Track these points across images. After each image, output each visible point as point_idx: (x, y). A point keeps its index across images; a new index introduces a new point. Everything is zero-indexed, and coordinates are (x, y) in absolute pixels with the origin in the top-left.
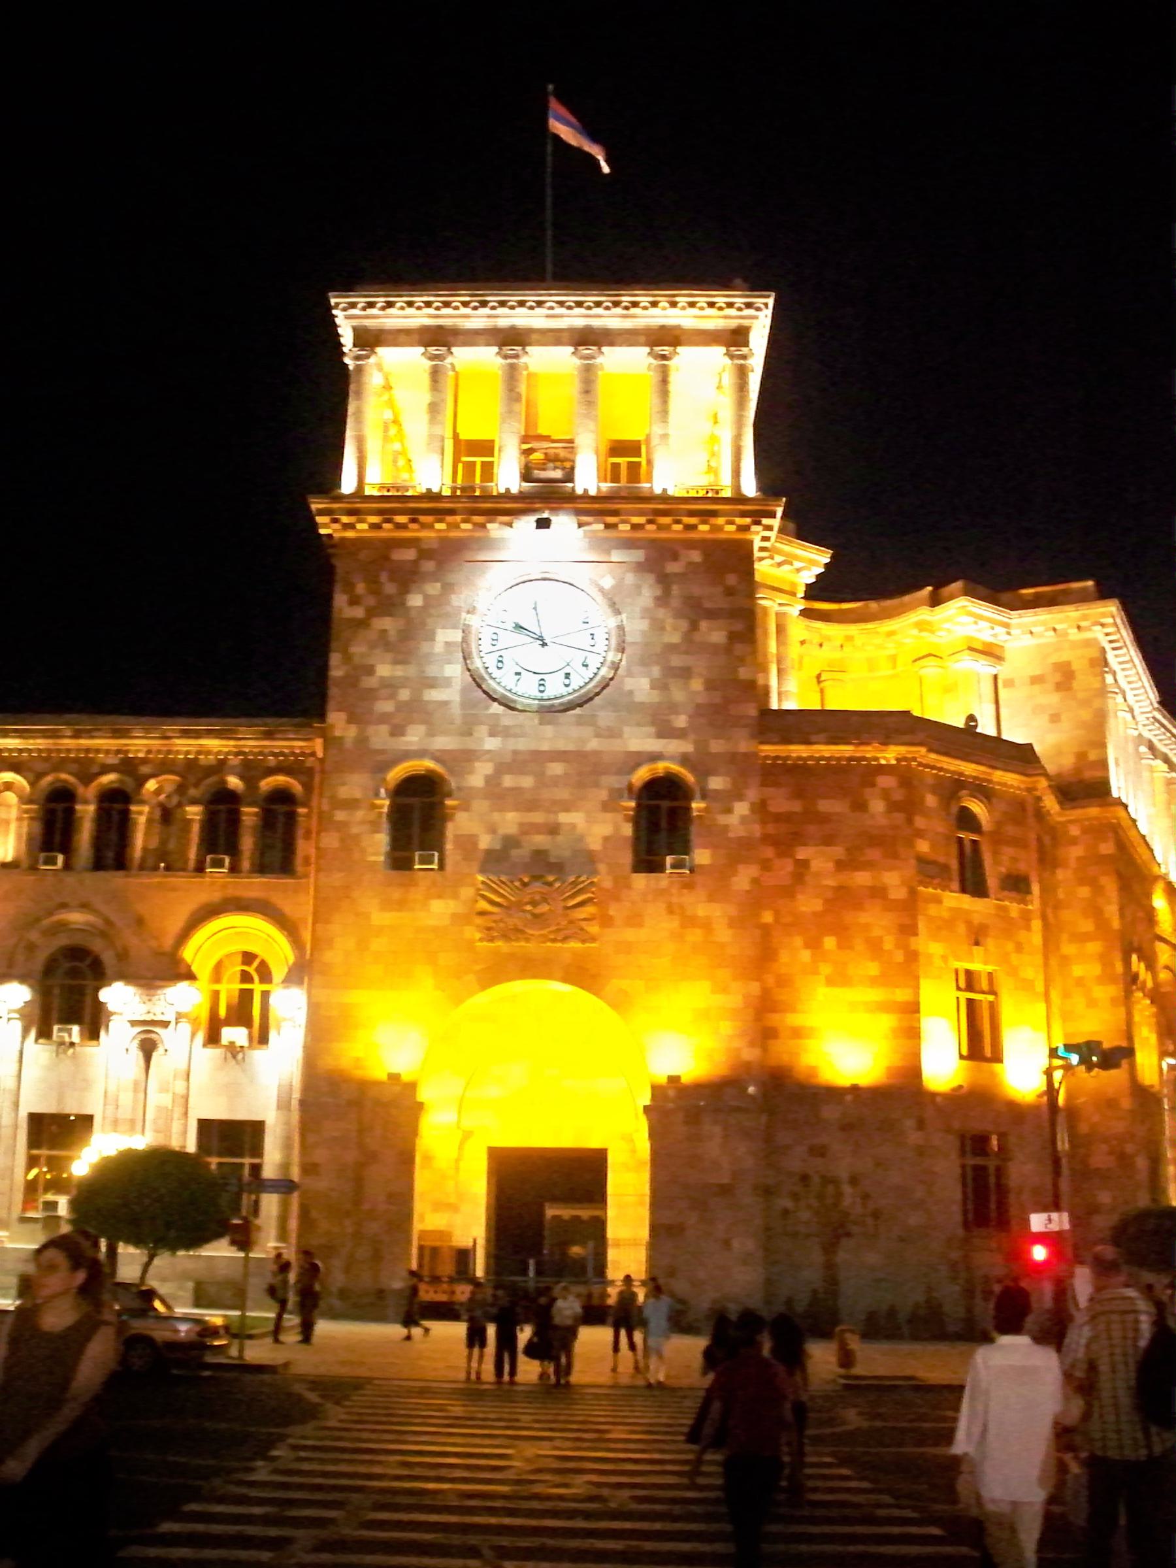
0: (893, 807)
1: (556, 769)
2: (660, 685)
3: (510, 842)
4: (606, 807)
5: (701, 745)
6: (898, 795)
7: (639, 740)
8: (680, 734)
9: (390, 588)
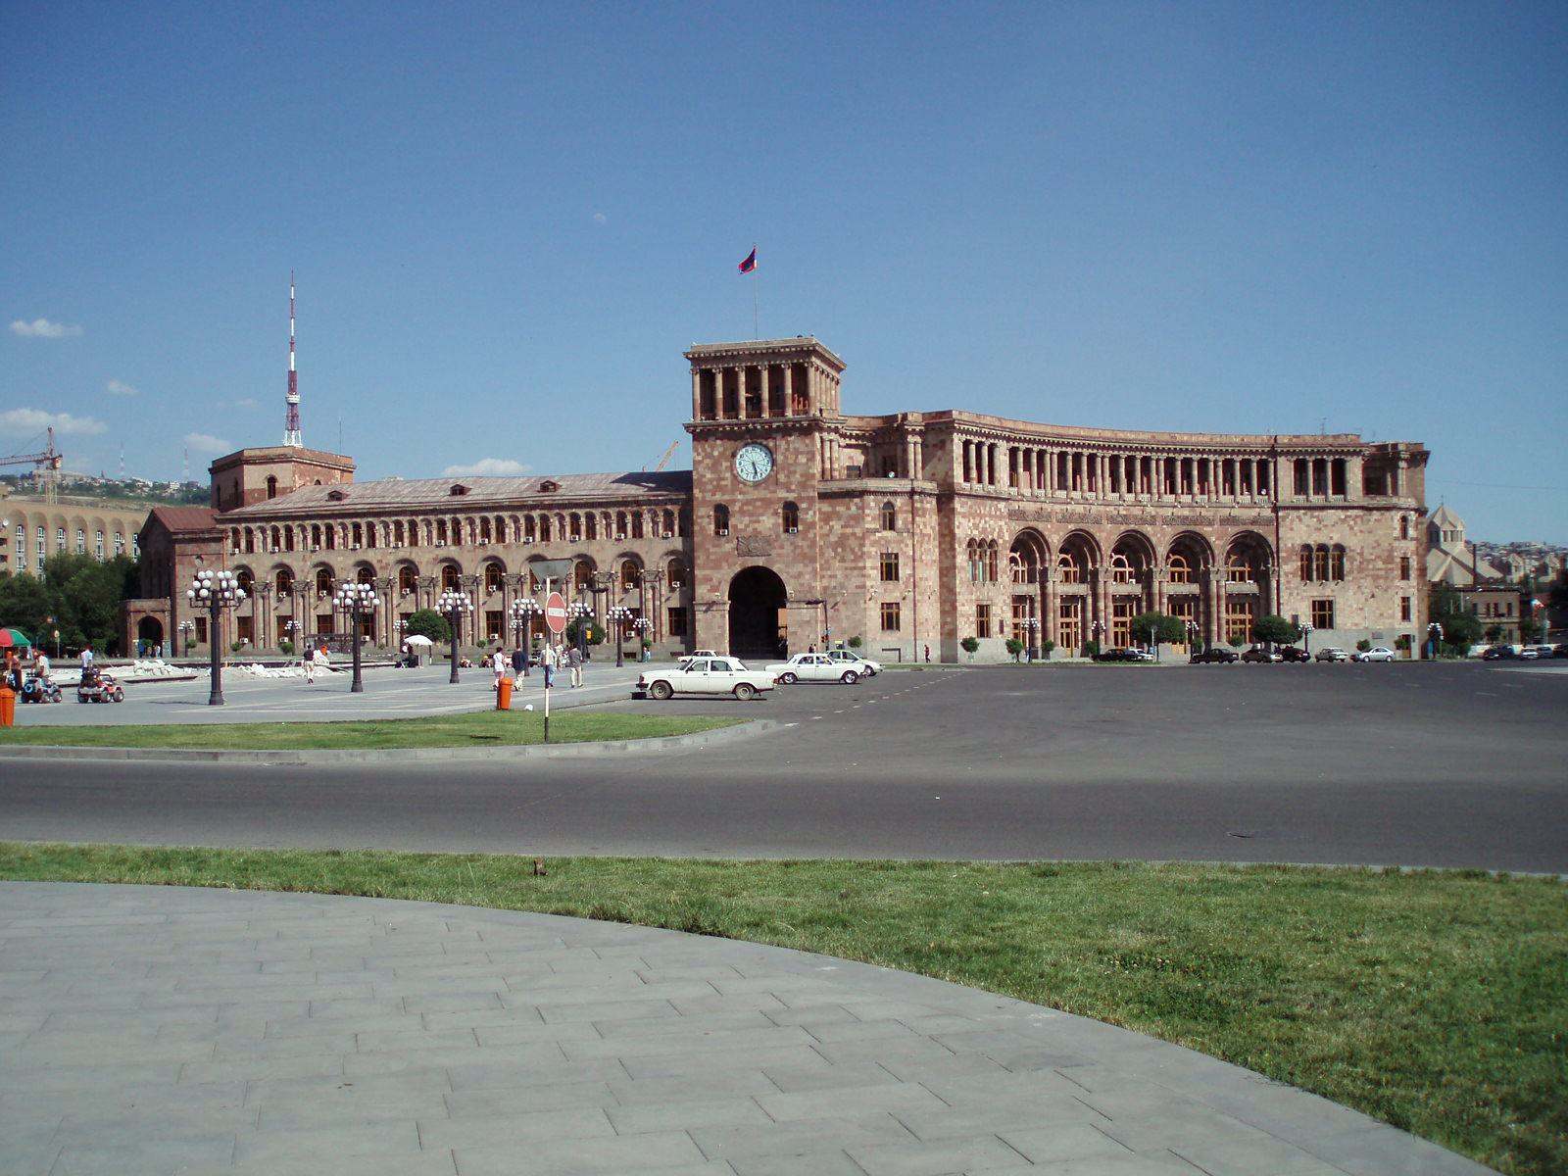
0: (858, 508)
1: (759, 504)
2: (787, 476)
3: (747, 526)
4: (773, 514)
5: (799, 494)
6: (860, 505)
7: (782, 494)
8: (793, 491)
9: (709, 450)
